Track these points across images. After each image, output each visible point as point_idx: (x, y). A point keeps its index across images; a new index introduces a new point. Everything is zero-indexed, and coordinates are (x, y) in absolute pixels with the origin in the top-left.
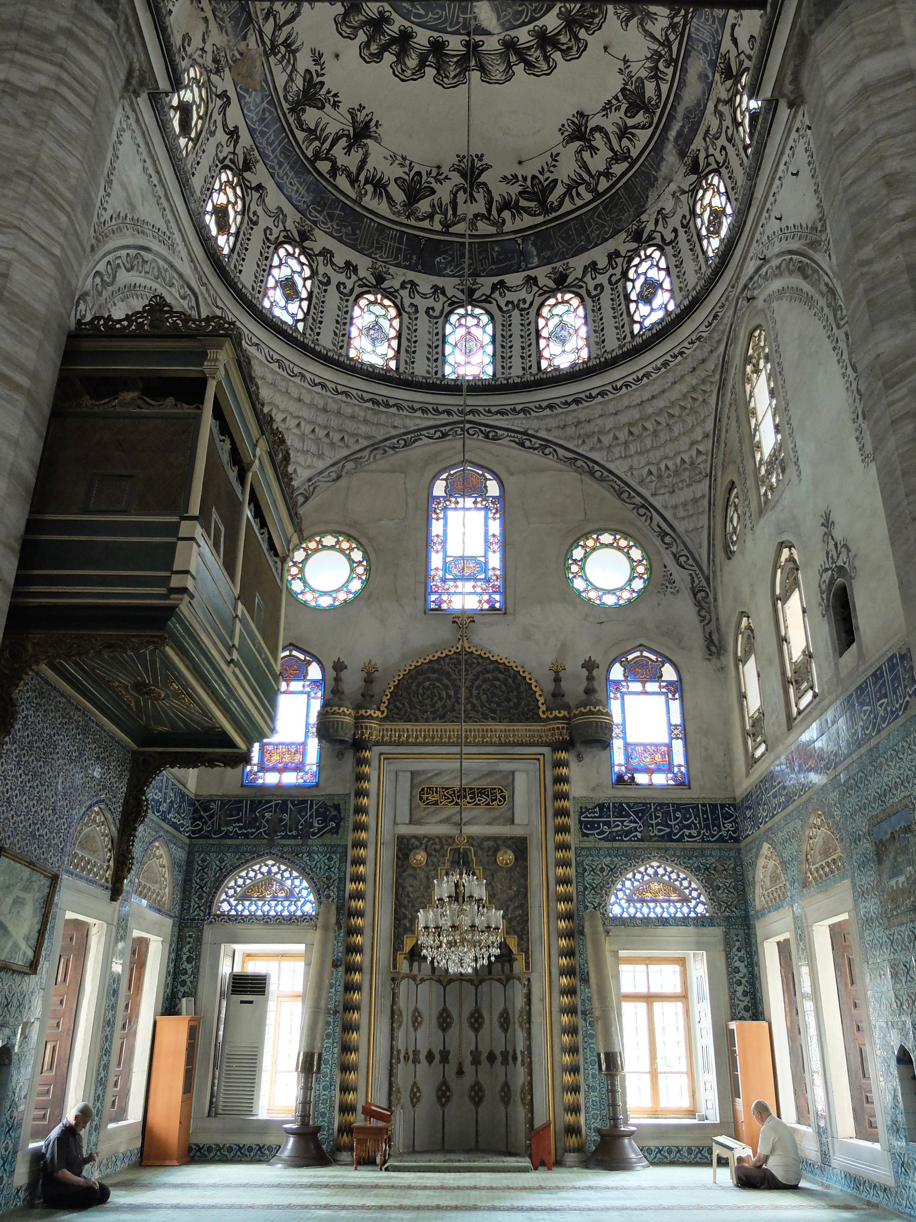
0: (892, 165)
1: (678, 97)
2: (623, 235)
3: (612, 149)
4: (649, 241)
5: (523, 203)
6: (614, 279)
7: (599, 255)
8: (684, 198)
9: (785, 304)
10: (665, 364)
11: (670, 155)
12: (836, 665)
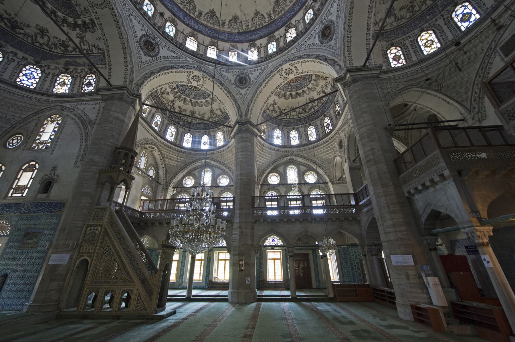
0: (114, 133)
1: (75, 57)
2: (33, 58)
3: (48, 43)
4: (40, 67)
5: (5, 20)
6: (20, 63)
7: (20, 54)
8: (58, 71)
9: (72, 122)
10: (23, 96)
11: (63, 61)
12: (37, 195)
